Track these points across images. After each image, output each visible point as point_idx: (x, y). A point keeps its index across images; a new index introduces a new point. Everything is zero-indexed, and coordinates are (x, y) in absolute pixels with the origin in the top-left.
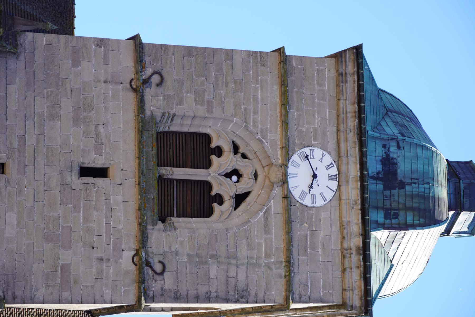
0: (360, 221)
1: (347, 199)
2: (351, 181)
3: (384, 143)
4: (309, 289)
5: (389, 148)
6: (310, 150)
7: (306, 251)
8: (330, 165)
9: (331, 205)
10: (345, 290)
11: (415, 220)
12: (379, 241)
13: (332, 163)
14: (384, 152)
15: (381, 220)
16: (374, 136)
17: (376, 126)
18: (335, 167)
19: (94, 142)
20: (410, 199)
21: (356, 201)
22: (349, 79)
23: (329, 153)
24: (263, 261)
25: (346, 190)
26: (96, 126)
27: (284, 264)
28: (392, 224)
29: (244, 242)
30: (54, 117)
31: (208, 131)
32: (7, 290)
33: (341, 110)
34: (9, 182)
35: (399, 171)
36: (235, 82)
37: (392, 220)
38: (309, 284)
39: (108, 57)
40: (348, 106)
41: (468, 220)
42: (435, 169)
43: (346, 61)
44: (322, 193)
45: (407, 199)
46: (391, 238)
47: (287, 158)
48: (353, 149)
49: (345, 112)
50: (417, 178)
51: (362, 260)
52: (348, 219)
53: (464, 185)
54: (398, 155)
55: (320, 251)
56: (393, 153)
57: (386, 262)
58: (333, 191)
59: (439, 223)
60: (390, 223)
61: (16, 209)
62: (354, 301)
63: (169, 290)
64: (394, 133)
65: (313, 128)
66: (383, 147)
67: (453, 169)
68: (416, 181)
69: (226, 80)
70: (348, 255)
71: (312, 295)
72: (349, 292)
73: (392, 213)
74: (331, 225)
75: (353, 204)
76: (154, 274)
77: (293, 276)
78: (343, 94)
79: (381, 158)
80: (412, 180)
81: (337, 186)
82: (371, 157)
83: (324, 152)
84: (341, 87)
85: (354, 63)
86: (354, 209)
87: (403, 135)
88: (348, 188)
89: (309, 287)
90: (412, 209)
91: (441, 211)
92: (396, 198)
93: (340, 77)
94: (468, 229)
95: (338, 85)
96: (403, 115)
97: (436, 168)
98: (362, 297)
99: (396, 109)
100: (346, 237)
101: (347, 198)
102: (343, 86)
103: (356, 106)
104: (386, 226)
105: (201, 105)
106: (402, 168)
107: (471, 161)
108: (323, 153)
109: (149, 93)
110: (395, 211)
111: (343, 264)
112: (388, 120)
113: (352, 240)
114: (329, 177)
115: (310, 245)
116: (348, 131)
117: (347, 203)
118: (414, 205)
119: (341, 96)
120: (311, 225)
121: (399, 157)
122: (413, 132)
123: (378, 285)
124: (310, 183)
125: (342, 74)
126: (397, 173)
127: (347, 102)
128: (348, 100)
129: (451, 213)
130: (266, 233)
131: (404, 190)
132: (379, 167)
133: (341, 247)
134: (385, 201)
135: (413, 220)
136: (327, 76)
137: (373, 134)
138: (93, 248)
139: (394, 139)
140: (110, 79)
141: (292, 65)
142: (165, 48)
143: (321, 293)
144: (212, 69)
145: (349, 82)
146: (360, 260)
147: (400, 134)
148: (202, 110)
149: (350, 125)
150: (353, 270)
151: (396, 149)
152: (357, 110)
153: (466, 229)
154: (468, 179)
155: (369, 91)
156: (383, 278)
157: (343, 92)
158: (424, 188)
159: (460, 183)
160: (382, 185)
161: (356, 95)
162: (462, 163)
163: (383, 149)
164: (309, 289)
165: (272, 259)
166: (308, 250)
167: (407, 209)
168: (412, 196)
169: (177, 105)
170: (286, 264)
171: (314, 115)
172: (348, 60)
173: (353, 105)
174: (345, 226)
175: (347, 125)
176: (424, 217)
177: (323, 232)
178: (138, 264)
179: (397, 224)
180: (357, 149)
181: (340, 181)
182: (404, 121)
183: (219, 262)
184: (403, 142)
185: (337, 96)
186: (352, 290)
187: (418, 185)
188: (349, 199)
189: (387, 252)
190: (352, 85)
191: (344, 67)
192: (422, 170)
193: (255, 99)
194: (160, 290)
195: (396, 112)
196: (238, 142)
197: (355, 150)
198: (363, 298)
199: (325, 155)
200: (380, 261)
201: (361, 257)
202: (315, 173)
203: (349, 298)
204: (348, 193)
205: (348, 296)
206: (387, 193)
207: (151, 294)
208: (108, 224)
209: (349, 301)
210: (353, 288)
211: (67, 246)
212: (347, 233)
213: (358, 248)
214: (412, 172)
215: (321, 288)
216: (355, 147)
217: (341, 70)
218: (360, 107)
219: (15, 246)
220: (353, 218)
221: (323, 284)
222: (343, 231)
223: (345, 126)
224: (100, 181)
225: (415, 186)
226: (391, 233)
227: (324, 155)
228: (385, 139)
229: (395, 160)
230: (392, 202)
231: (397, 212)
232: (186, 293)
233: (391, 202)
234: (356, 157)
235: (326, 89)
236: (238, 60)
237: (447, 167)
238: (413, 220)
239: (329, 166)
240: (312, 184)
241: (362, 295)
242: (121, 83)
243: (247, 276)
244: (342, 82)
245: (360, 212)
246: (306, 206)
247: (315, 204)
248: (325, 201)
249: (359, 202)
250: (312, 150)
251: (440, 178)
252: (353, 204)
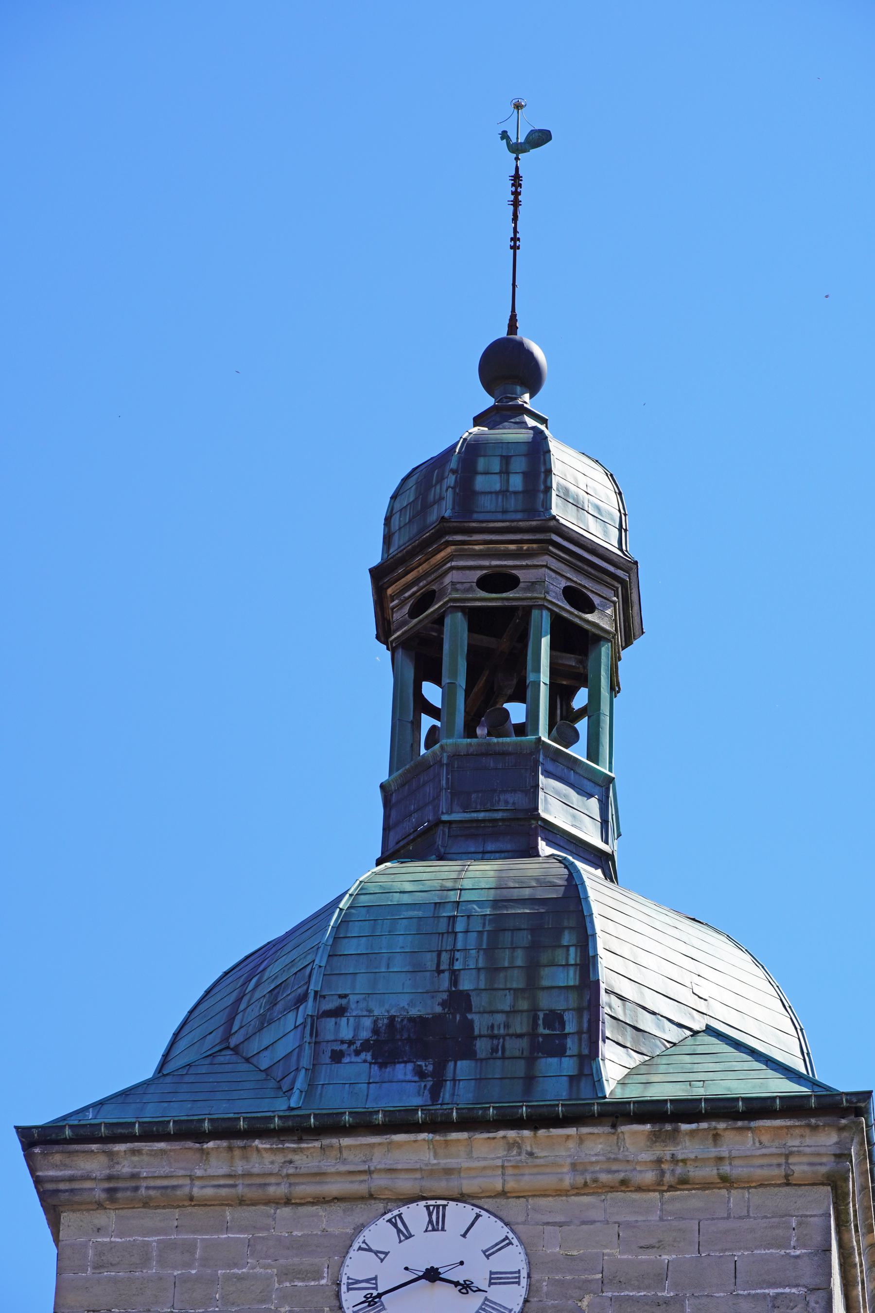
0: (572, 1131)
1: (503, 1174)
2: (445, 1162)
3: (326, 1058)
4: (787, 1290)
5: (343, 1042)
6: (349, 1289)
7: (667, 1302)
8: (395, 1225)
9: (524, 1223)
10: (787, 1176)
11: (567, 959)
12: (633, 1072)
13: (389, 1221)
14: (354, 1059)
15: (568, 1066)
16: (305, 1087)
17: (272, 1084)
18: (403, 1210)
20: (502, 975)
21: (508, 1143)
22: (125, 1168)
23: (359, 1229)
25: (474, 1177)
28: (579, 1033)
33: (224, 1192)
35: (414, 1012)
37: (567, 1031)
38: (772, 1292)
40: (211, 1172)
41: (566, 796)
42: (406, 899)
43: (71, 1179)
44: (484, 1252)
45: (502, 986)
46: (623, 1035)
48: (345, 1154)
49: (231, 1182)
50: (435, 954)
51: (694, 1126)
52: (565, 1170)
53: (456, 808)
54: (365, 1013)
55: (666, 1257)
56: (357, 1028)
57: (700, 1049)
58: (478, 1216)
59: (576, 885)
60: (576, 1036)
62: (823, 1150)
64: (296, 1027)
65: (279, 1282)
66: (339, 1062)
67: (408, 844)
68: (445, 957)
70: (679, 1170)
71: (807, 1280)
72: (794, 1164)
73: (547, 1032)
74: (584, 1223)
75: (519, 1154)
78: (174, 1188)
79: (375, 1068)
80: (443, 971)
81: (461, 1205)
82: (371, 1097)
83: (356, 1246)
84: (152, 1193)
85: (77, 1151)
86: (535, 1150)
87: (302, 999)
88: (469, 1169)
90: (532, 969)
91: (537, 880)
92: (500, 1018)
93: (119, 1195)
94: (590, 796)
96: (239, 1000)
97: (406, 895)
98: (809, 1126)
99: (222, 1018)
100: (621, 1176)
101: (500, 1173)
102: (147, 1188)
103: (211, 1144)
104: (586, 1052)
106: (404, 1001)
107: (382, 786)
108: (360, 1249)
110: (540, 1022)
111: (706, 1186)
112: (254, 1047)
113: (631, 1158)
114: (434, 1230)
115: (648, 1288)
116: (291, 1171)
117: (516, 1171)
118: (519, 962)
119: (179, 1192)
120: (585, 1287)
121: (370, 1011)
122: (293, 966)
123: (771, 1073)
124: (453, 1291)
125: (111, 1191)
126: (420, 1017)
127: (199, 1173)
128: (192, 1170)
129: (544, 849)
131: (473, 994)
132: (403, 1071)
133: (654, 1191)
134: (507, 1054)
135: (568, 965)
136: (117, 1236)
137: (298, 1091)
139: (314, 1024)
143: (798, 1252)
145: (135, 1167)
146: (692, 1133)
147: (298, 1008)
149: (272, 1163)
150: (725, 1154)
151: (344, 1020)
152: (224, 1144)
153: (593, 804)
154: (438, 797)
155: (165, 1105)
156: (750, 1058)
157: (165, 1188)
158: (467, 932)
159: (450, 822)
160: (459, 1063)
161: (176, 1146)
162: (390, 815)
163: (346, 1060)
164: (787, 1290)
166: (665, 1294)
167: (532, 986)
168: (493, 970)
171: (241, 1278)
172: (68, 1173)
173: (208, 1153)
174: (588, 1177)
175: (271, 1174)
176: (558, 932)
177: (606, 1247)
179: (580, 1017)
180: (346, 1141)
181: (446, 1194)
182: (257, 995)
184: (324, 997)
185: (178, 1207)
186: (787, 1156)
187: (458, 950)
188: (503, 1167)
189: (668, 1045)
190: (146, 1158)
191: (88, 1185)
192: (410, 938)
195: (231, 1020)
197: (349, 1147)
198: (813, 1121)
199: (364, 1242)
200: (697, 1068)
201: (684, 1127)
202: (421, 1274)
203: (811, 1164)
204: (484, 1168)
205: (806, 1168)
206: (482, 1047)
209: (821, 1164)
210: (780, 1155)
212: (609, 1172)
213: (655, 1138)
214: (417, 970)
215: (782, 1252)
216: (340, 1149)
217: (100, 1195)
218: (216, 1134)
220: (564, 1153)
222: (604, 1186)
223: (273, 1180)
225: (461, 960)
226: (608, 1034)
227: (364, 1246)
228: (316, 1055)
229: (380, 1023)
230: (511, 1031)
231: (541, 1015)
233: (511, 1035)
234: (372, 1146)
235: (158, 1242)
237: (402, 863)
238: (568, 965)
239: (399, 1231)
240: (457, 1284)
241: (803, 1123)
244: (136, 1189)
245: (542, 1132)
246: (526, 1301)
247: (519, 1272)
248: (511, 1243)
249: (512, 1134)
250: (348, 1284)
251: (436, 884)
252: (519, 1154)
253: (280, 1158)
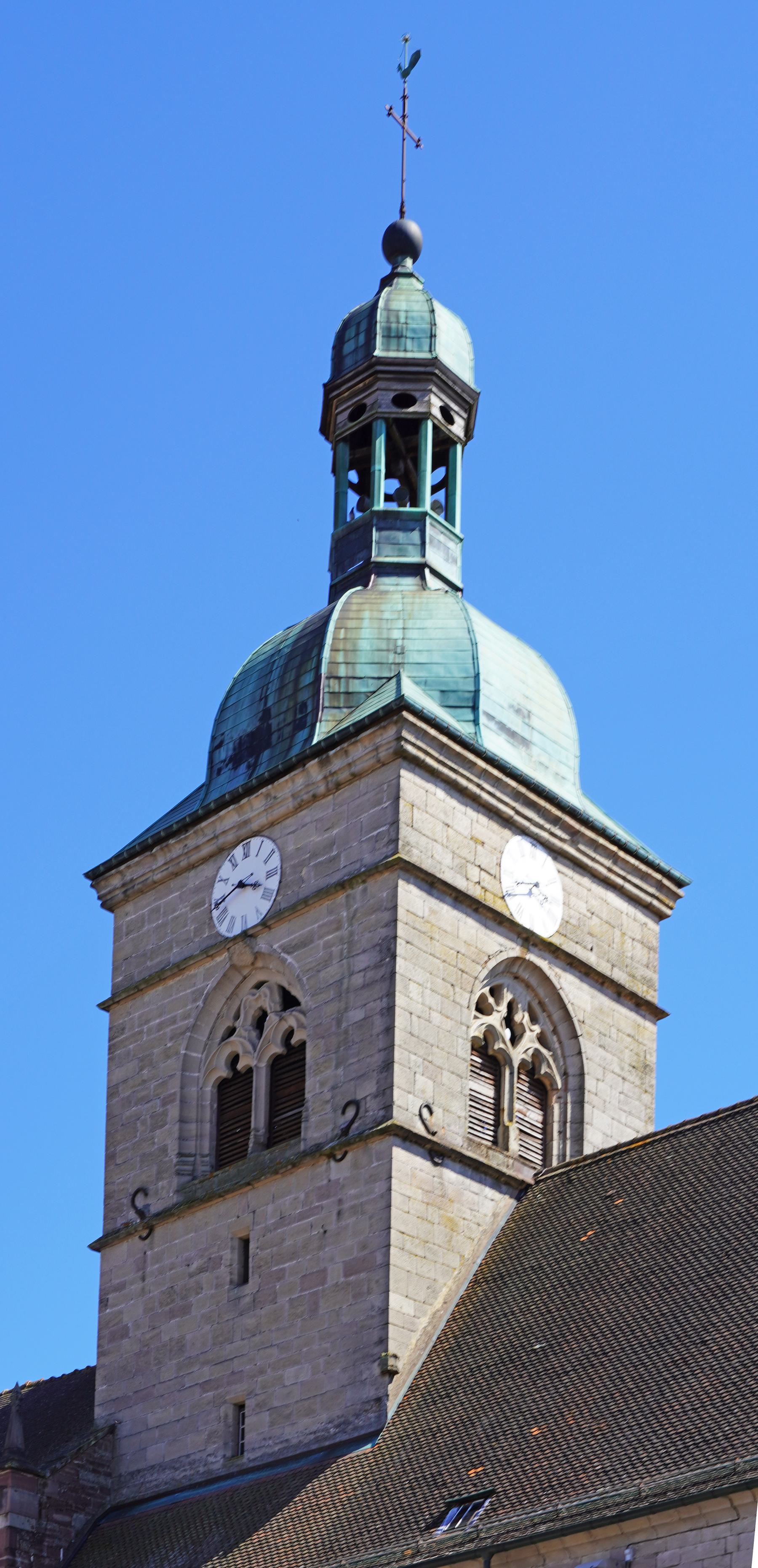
0: (287, 777)
9: (280, 837)
19: (208, 1274)
22: (128, 878)
24: (344, 932)
26: (191, 1276)
27: (350, 891)
29: (322, 974)
30: (180, 1346)
31: (209, 1089)
32: (372, 1356)
34: (251, 1392)
36: (141, 1069)
38: (375, 833)
39: (118, 1284)
43: (110, 892)
47: (226, 943)
55: (335, 832)
61: (280, 1372)
62: (390, 739)
63: (377, 1083)
69: (139, 1085)
74: (303, 826)
76: (359, 1117)
77: (365, 866)
78: (147, 879)
83: (218, 879)
85: (110, 876)
89: (379, 831)
95: (142, 892)
100: (311, 793)
103: (154, 850)
105: (167, 1115)
109: (156, 1207)
119: (149, 881)
127: (154, 867)
130: (312, 941)
138: (325, 1232)
140: (140, 1274)
141: (122, 981)
144: (128, 1113)
146: (335, 754)
157: (143, 882)
164: (381, 829)
165: (343, 915)
169: (167, 1155)
170: (348, 887)
178: (344, 1150)
180: (203, 824)
183: (346, 1009)
193: (160, 1027)
194: (378, 1099)
196: (220, 1032)
201: (331, 753)
207: (382, 1113)
208: (302, 1216)
219: (321, 1361)
221: (375, 807)
222: (309, 802)
232: (382, 1053)
240: (251, 885)
242: (145, 1253)
243: (364, 951)
245: (276, 783)
249: (264, 790)
253: (181, 845)
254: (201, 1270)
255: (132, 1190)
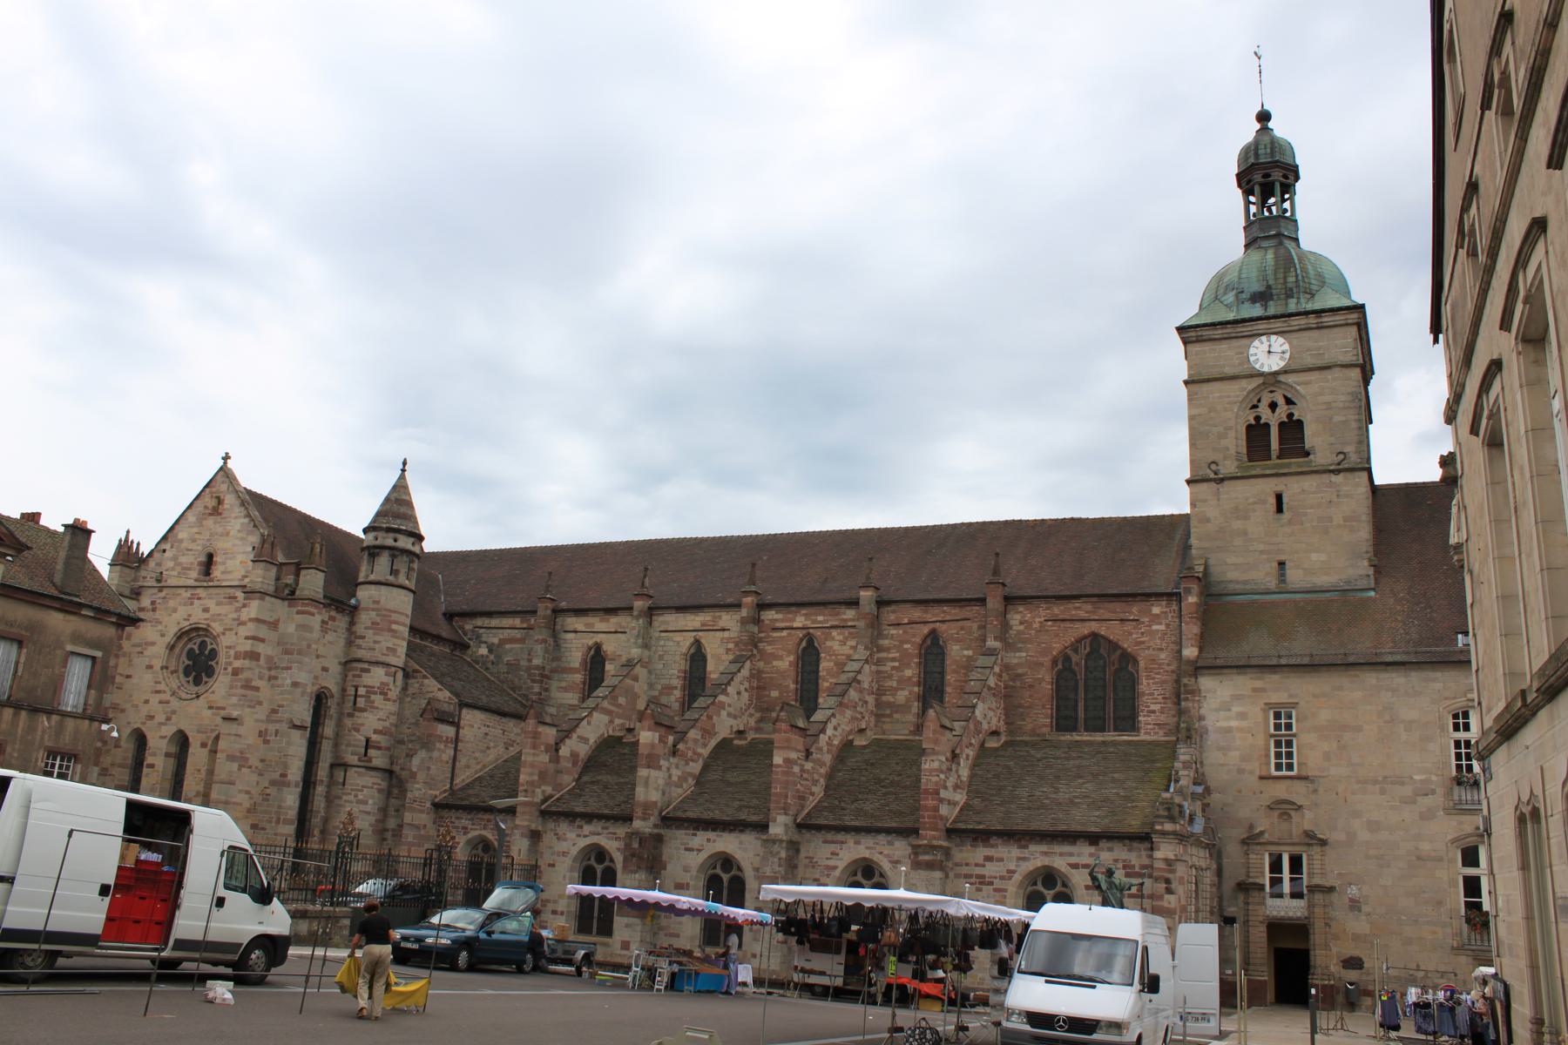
30: (1245, 533)
142: (1192, 462)
148: (1232, 434)
208: (1314, 493)
211: (1330, 519)
224: (1285, 500)
236: (1196, 411)
254: (1255, 503)
255: (1211, 460)
